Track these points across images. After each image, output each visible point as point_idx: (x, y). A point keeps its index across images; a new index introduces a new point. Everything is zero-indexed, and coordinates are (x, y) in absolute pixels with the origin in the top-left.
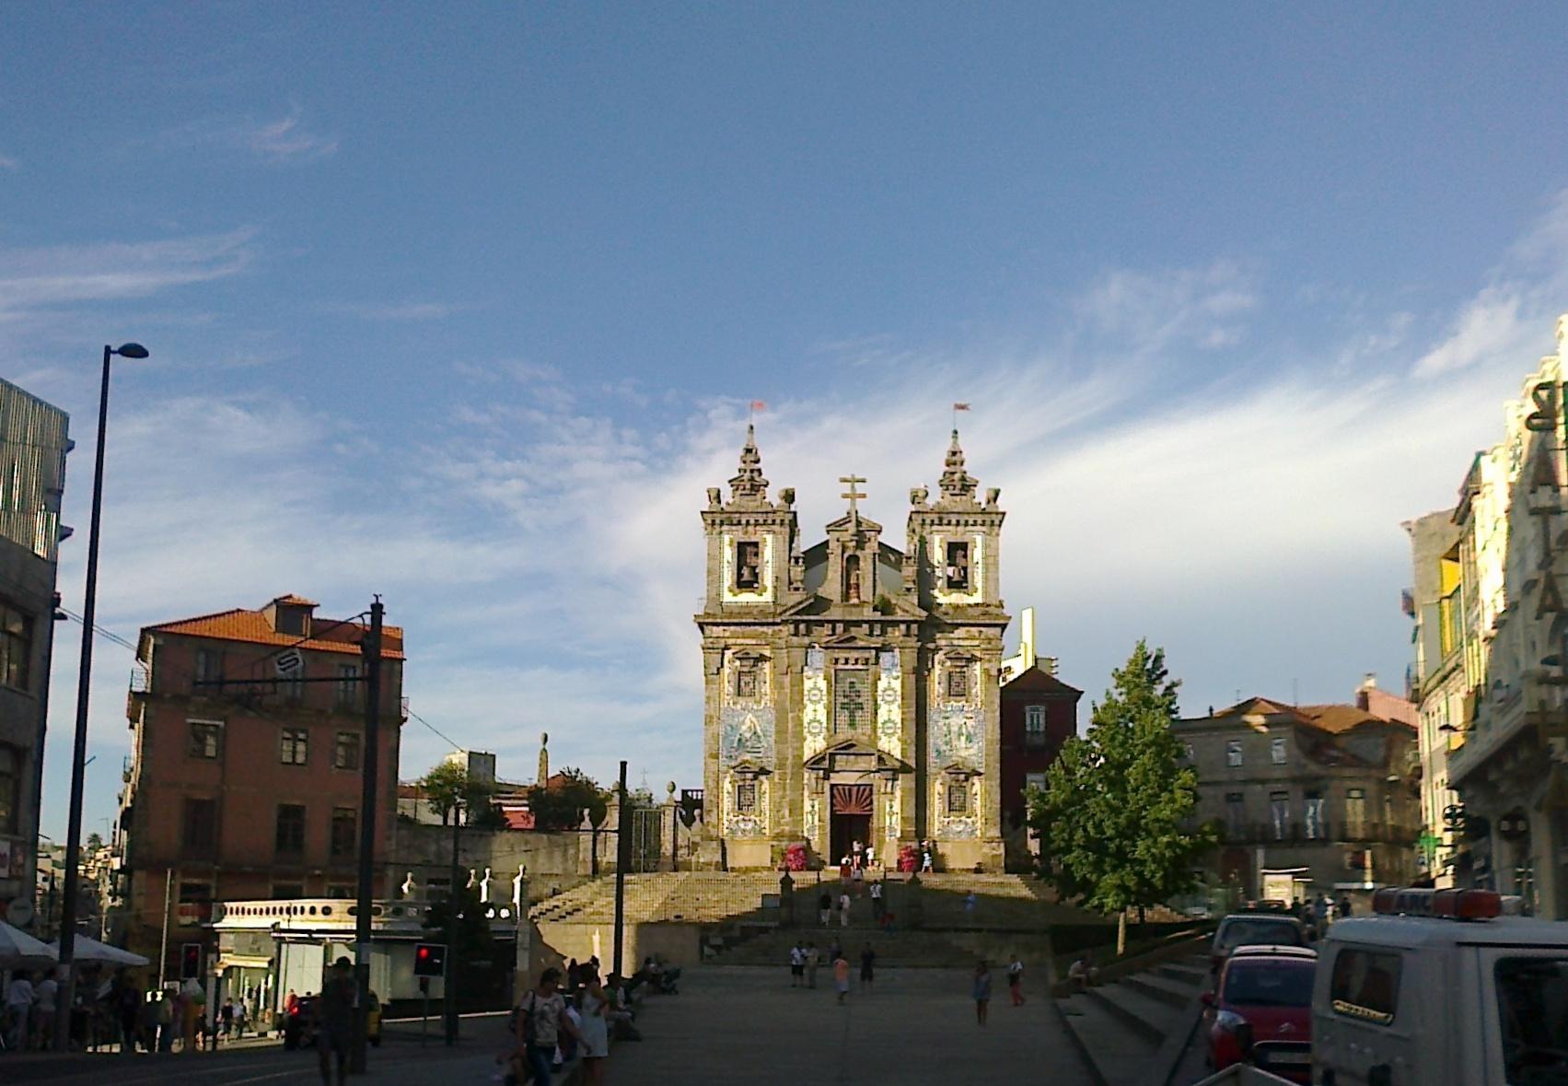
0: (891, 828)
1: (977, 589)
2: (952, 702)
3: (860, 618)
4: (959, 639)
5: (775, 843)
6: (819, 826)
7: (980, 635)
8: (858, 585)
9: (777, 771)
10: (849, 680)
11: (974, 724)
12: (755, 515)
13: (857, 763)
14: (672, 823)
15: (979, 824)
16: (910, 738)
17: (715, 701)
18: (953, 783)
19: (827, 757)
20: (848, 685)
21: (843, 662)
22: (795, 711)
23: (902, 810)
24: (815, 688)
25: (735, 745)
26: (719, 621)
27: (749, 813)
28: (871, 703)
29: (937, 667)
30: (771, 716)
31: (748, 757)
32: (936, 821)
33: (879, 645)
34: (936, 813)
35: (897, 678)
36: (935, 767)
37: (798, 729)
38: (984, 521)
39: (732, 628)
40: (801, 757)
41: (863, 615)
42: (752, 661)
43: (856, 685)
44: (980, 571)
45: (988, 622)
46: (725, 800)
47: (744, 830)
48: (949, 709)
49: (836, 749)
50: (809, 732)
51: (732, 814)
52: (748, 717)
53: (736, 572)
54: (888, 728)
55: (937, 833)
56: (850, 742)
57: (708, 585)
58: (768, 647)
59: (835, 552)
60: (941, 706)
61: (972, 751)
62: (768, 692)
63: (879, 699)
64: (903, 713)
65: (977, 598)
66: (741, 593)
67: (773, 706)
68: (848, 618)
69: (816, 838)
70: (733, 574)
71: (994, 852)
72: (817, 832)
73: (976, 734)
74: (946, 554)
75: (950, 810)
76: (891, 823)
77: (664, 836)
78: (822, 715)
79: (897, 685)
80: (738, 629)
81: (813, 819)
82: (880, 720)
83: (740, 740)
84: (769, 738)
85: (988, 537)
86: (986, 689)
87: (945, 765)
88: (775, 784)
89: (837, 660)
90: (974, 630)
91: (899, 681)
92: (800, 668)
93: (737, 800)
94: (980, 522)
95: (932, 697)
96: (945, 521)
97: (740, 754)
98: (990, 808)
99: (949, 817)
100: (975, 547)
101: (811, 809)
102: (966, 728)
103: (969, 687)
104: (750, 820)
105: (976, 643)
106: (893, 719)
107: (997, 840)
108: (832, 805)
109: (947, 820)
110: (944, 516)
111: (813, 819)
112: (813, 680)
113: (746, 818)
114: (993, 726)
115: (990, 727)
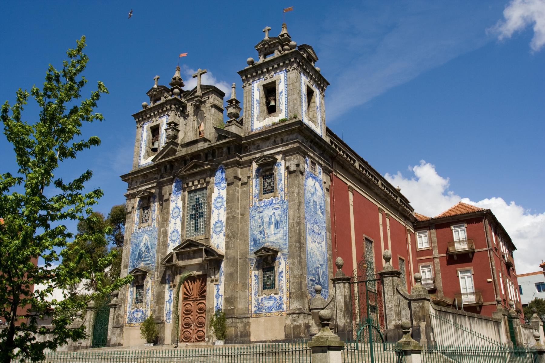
1: (282, 110)
2: (264, 199)
3: (196, 150)
4: (268, 150)
9: (156, 273)
11: (280, 212)
15: (284, 299)
16: (231, 232)
21: (190, 184)
22: (164, 227)
23: (225, 292)
25: (137, 258)
32: (253, 299)
34: (253, 293)
37: (165, 239)
46: (129, 297)
47: (136, 319)
48: (263, 204)
52: (144, 238)
54: (217, 227)
55: (253, 310)
60: (257, 203)
63: (213, 206)
64: (228, 214)
68: (189, 152)
69: (171, 320)
71: (295, 323)
72: (171, 316)
73: (281, 221)
79: (224, 193)
81: (170, 305)
82: (213, 222)
83: (139, 253)
84: (153, 250)
85: (289, 73)
86: (289, 183)
91: (225, 190)
93: (135, 297)
94: (281, 64)
98: (293, 283)
99: (262, 295)
101: (169, 298)
102: (275, 218)
103: (276, 185)
104: (140, 311)
106: (221, 220)
107: (297, 312)
109: (260, 298)
111: (170, 305)
112: (175, 202)
113: (138, 310)
114: (294, 211)
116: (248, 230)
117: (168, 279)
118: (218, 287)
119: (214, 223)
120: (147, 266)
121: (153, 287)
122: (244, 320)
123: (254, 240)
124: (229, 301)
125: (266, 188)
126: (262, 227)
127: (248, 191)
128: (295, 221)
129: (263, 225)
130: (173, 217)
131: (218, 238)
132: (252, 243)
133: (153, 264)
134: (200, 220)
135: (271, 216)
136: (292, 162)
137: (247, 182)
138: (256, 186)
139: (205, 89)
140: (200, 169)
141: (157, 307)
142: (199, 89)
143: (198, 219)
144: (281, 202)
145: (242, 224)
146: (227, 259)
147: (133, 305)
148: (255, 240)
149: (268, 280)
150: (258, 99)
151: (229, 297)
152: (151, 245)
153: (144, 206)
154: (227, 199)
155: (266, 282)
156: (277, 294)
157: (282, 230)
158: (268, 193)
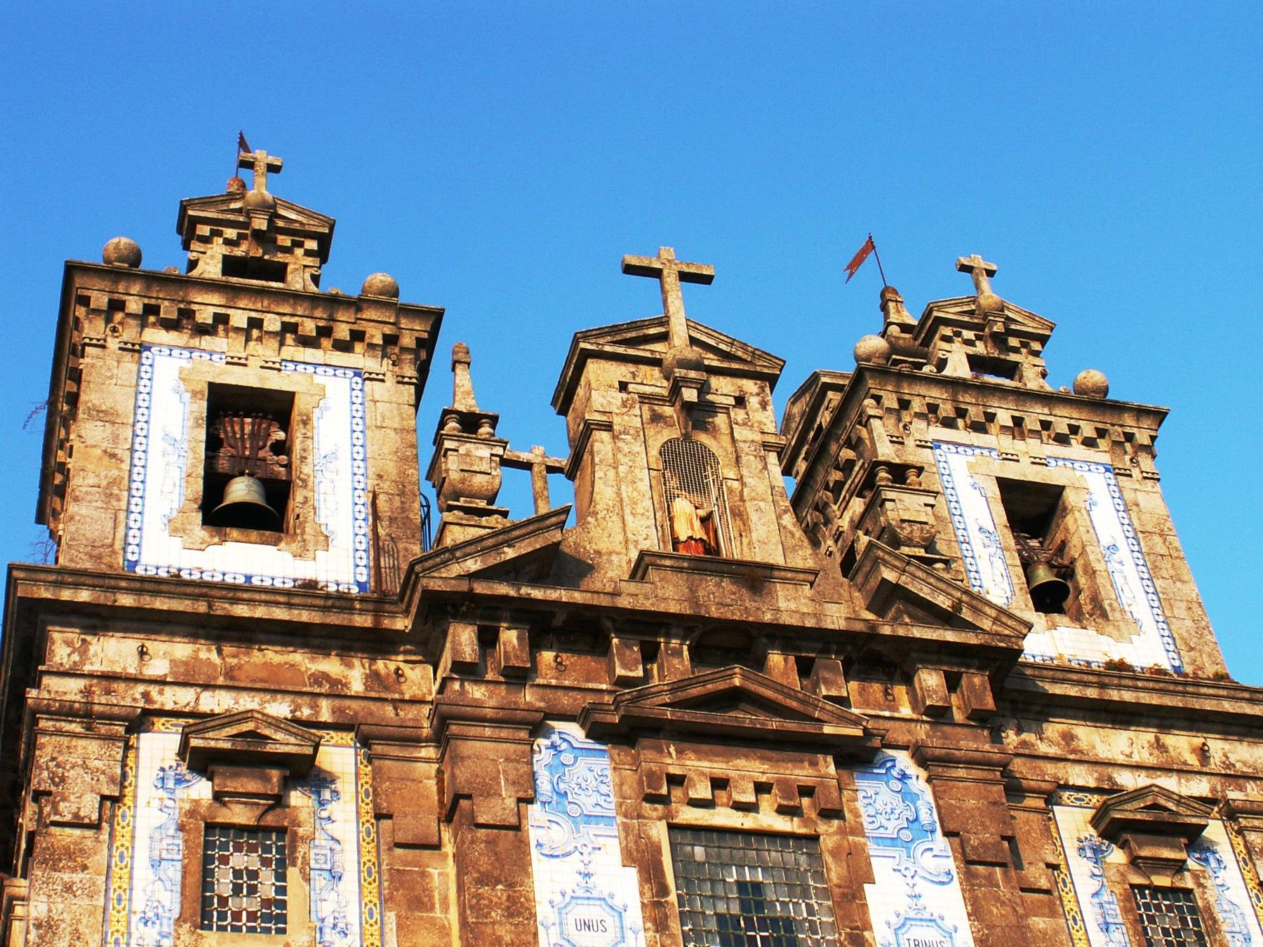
3: (768, 617)
7: (1202, 766)
10: (732, 877)
12: (287, 310)
21: (702, 791)
26: (126, 600)
29: (1081, 870)
38: (1102, 433)
39: (182, 649)
41: (778, 610)
43: (770, 895)
45: (1228, 706)
58: (348, 737)
59: (616, 420)
62: (353, 918)
66: (223, 540)
68: (714, 612)
80: (208, 653)
91: (954, 891)
92: (511, 803)
94: (1088, 430)
96: (975, 413)
105: (1200, 787)
110: (966, 398)
112: (575, 861)
127: (1064, 937)
137: (1048, 892)
138: (1106, 927)
140: (791, 725)
150: (992, 529)
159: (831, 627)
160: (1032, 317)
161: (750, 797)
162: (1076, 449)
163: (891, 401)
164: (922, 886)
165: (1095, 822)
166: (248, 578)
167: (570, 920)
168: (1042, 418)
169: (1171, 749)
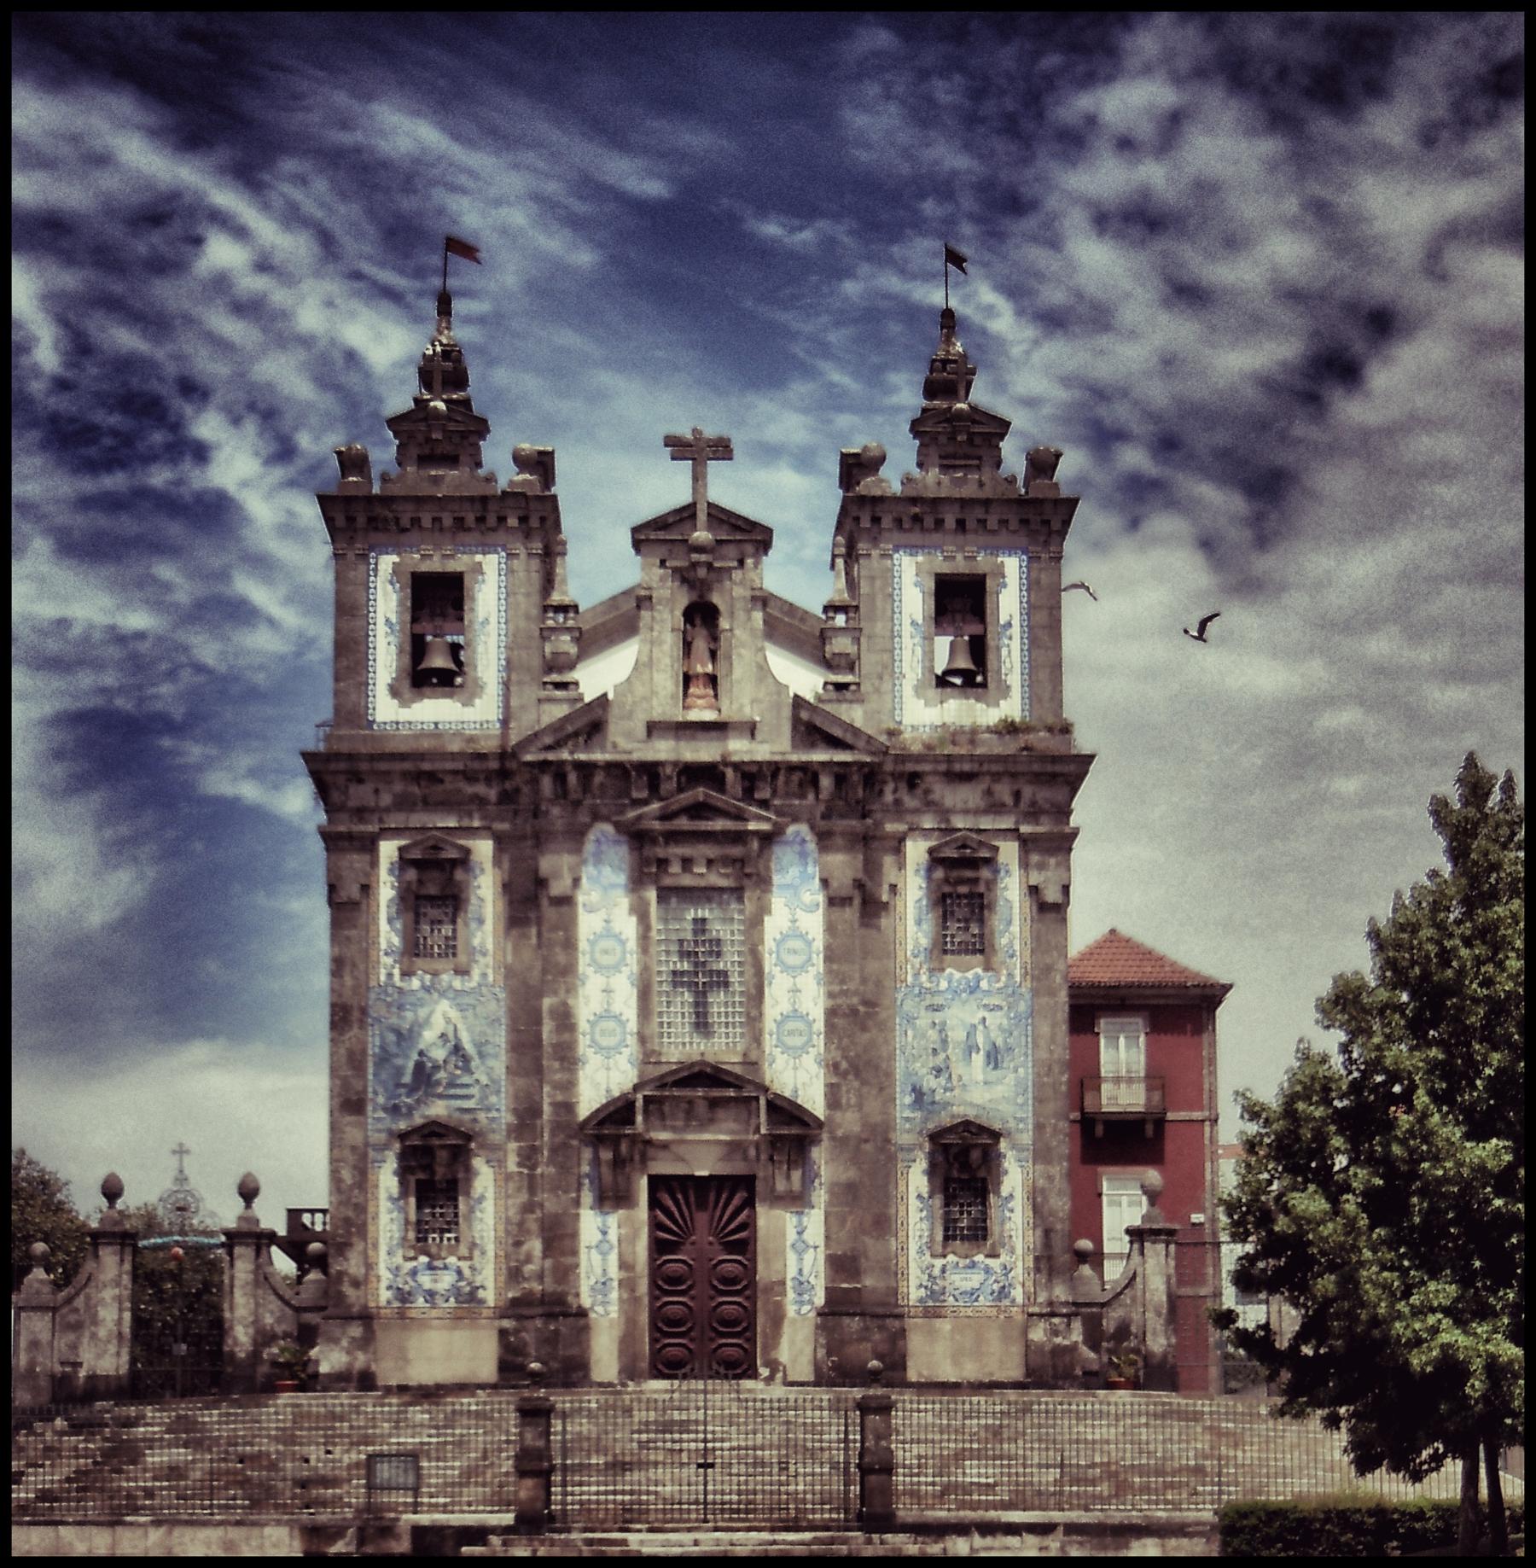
0: (802, 1286)
1: (1008, 687)
2: (949, 970)
4: (966, 812)
5: (507, 1324)
6: (620, 1282)
8: (712, 680)
9: (513, 1146)
11: (1005, 1022)
12: (456, 507)
13: (712, 1121)
14: (251, 1276)
16: (845, 1057)
17: (354, 965)
18: (955, 1174)
19: (639, 1103)
20: (689, 927)
21: (675, 868)
23: (827, 1238)
24: (608, 933)
27: (443, 1254)
28: (749, 971)
30: (496, 1006)
31: (438, 1109)
32: (912, 1265)
33: (765, 827)
34: (913, 1248)
35: (811, 909)
36: (908, 1131)
39: (398, 787)
40: (568, 1107)
42: (448, 866)
44: (1016, 645)
47: (431, 1295)
48: (944, 985)
49: (663, 1086)
50: (594, 1043)
51: (400, 1253)
53: (408, 648)
54: (791, 1033)
56: (696, 1069)
57: (337, 679)
61: (1000, 1091)
62: (490, 946)
64: (831, 995)
65: (1012, 707)
66: (422, 696)
67: (500, 978)
69: (614, 1311)
70: (400, 652)
71: (1058, 1340)
72: (614, 1295)
73: (1010, 1049)
74: (932, 602)
75: (946, 1238)
76: (800, 1271)
77: (232, 1309)
78: (626, 1002)
79: (814, 923)
80: (415, 790)
83: (419, 1066)
84: (491, 1062)
87: (931, 1126)
88: (508, 1177)
89: (663, 863)
90: (1004, 792)
92: (568, 881)
93: (413, 1217)
94: (1014, 524)
95: (900, 955)
97: (418, 1101)
99: (945, 1256)
100: (1005, 585)
101: (599, 1236)
102: (987, 1036)
103: (992, 933)
104: (446, 1267)
105: (1006, 823)
108: (655, 1225)
109: (939, 1263)
112: (602, 914)
114: (1054, 1026)
115: (1045, 1029)
116: (891, 1057)
117: (587, 1176)
118: (800, 1222)
119: (779, 1018)
120: (467, 1117)
121: (502, 1195)
122: (888, 1321)
123: (914, 1090)
124: (842, 1264)
125: (953, 936)
126: (942, 1056)
128: (1056, 1056)
129: (945, 1050)
130: (600, 968)
131: (795, 1068)
132: (908, 1100)
133: (494, 1114)
134: (717, 1001)
135: (974, 1026)
136: (1049, 874)
138: (919, 922)
139: (722, 521)
141: (548, 1263)
142: (702, 516)
143: (704, 994)
144: (1010, 990)
145: (867, 1036)
146: (833, 1138)
147: (413, 1247)
148: (919, 1094)
149: (962, 1213)
151: (845, 1255)
152: (480, 1046)
153: (423, 892)
154: (828, 948)
155: (956, 1221)
156: (993, 1255)
157: (1012, 1076)
158: (959, 952)
159: (759, 758)
160: (994, 418)
161: (704, 870)
162: (1004, 537)
163: (866, 523)
164: (800, 914)
165: (931, 851)
166: (436, 724)
167: (597, 949)
168: (980, 516)
169: (997, 796)
